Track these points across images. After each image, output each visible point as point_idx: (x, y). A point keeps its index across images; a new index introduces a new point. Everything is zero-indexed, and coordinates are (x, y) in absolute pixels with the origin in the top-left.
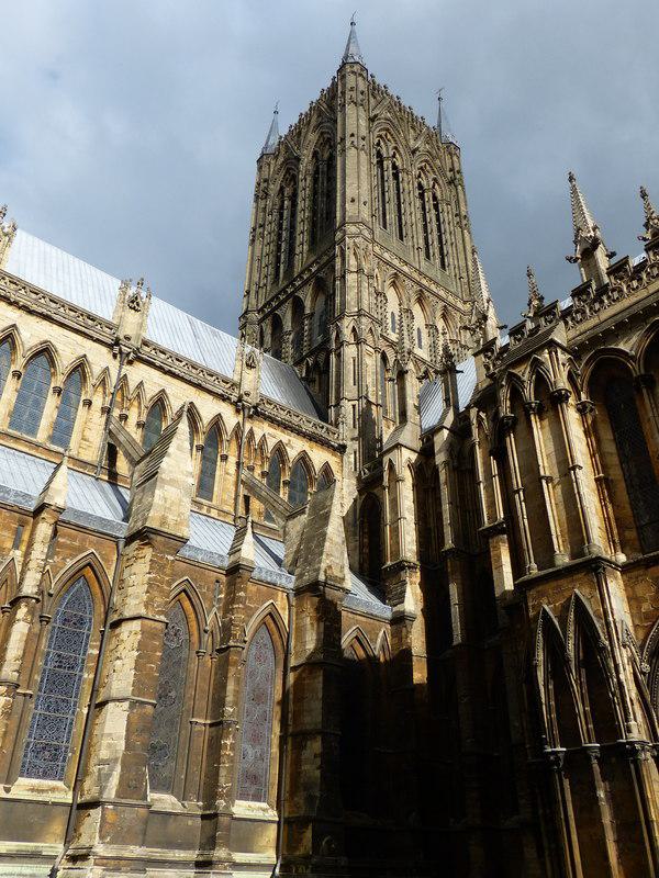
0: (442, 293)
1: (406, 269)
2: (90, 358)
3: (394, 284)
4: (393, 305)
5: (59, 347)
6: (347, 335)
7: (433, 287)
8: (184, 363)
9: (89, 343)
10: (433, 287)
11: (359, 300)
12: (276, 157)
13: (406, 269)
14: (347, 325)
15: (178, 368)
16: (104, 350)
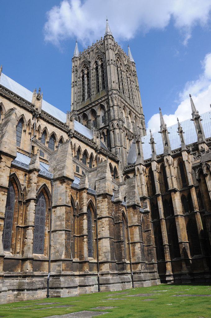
0: (135, 111)
1: (126, 104)
2: (63, 136)
3: (124, 109)
4: (124, 116)
5: (56, 133)
6: (116, 126)
7: (133, 110)
8: (83, 137)
9: (62, 132)
10: (133, 110)
11: (118, 115)
12: (80, 59)
13: (126, 104)
14: (115, 123)
15: (82, 139)
16: (66, 134)
